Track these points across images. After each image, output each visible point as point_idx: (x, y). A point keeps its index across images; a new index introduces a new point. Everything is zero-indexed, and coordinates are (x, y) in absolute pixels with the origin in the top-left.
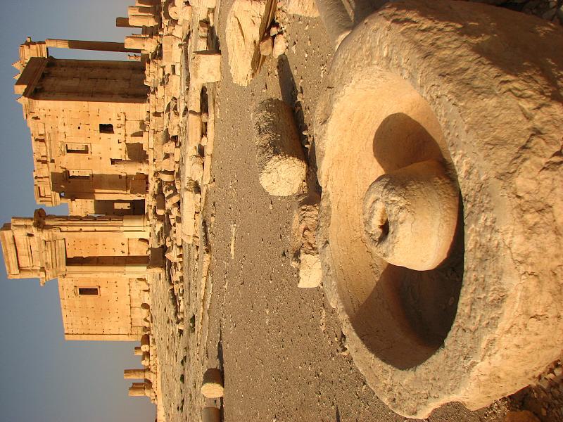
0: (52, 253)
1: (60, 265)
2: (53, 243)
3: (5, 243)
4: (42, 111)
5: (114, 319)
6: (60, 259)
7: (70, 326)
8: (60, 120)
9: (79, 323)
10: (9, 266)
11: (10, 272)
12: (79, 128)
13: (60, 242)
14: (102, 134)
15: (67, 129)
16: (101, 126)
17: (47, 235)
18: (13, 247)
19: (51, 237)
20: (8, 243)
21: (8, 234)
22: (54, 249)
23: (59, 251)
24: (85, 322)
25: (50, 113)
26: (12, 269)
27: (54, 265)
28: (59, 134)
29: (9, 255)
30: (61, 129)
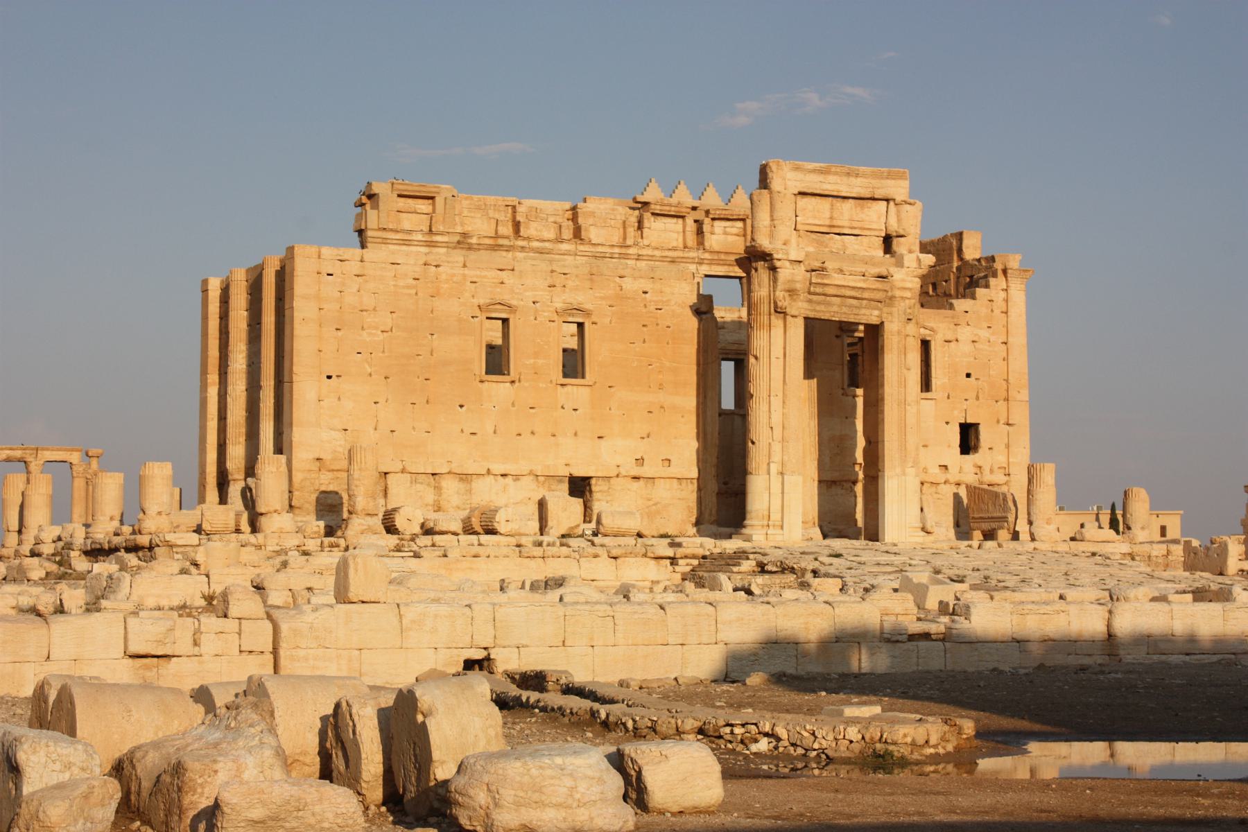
0: (854, 288)
1: (810, 301)
2: (879, 296)
3: (880, 176)
4: (1003, 295)
6: (829, 304)
7: (355, 267)
8: (984, 334)
9: (368, 301)
10: (814, 171)
11: (797, 169)
12: (968, 375)
13: (876, 313)
14: (958, 429)
15: (965, 347)
16: (975, 426)
17: (909, 285)
18: (865, 193)
19: (898, 293)
20: (875, 182)
21: (899, 189)
22: (866, 295)
23: (851, 306)
24: (369, 319)
25: (997, 312)
26: (799, 175)
27: (818, 290)
28: (952, 326)
29: (845, 179)
30: (965, 333)
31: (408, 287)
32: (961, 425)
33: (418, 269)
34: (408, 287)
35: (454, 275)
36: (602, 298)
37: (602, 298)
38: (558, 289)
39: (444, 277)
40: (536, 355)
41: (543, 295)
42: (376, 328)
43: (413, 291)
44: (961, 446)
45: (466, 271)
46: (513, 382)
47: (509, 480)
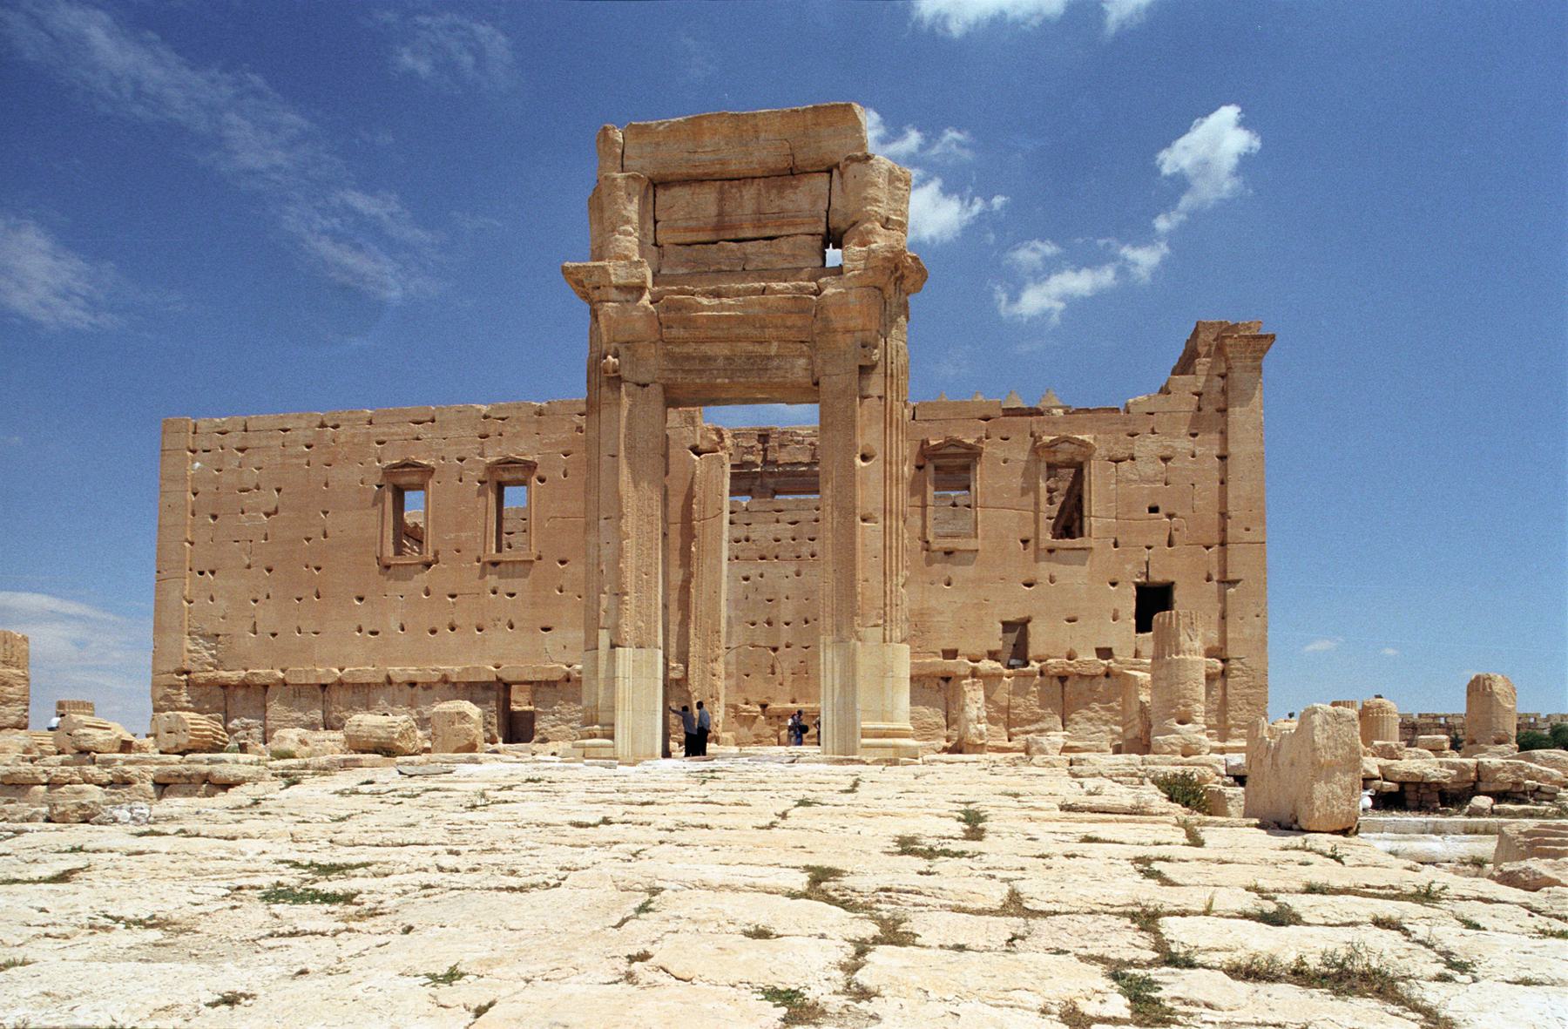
5: (267, 616)
7: (235, 439)
9: (250, 476)
14: (1133, 591)
31: (297, 457)
32: (1140, 588)
33: (309, 433)
34: (297, 457)
35: (354, 436)
36: (551, 445)
37: (551, 445)
38: (492, 438)
39: (342, 439)
40: (460, 527)
41: (470, 449)
42: (257, 510)
43: (305, 461)
44: (1137, 617)
45: (372, 429)
46: (428, 565)
47: (419, 690)
